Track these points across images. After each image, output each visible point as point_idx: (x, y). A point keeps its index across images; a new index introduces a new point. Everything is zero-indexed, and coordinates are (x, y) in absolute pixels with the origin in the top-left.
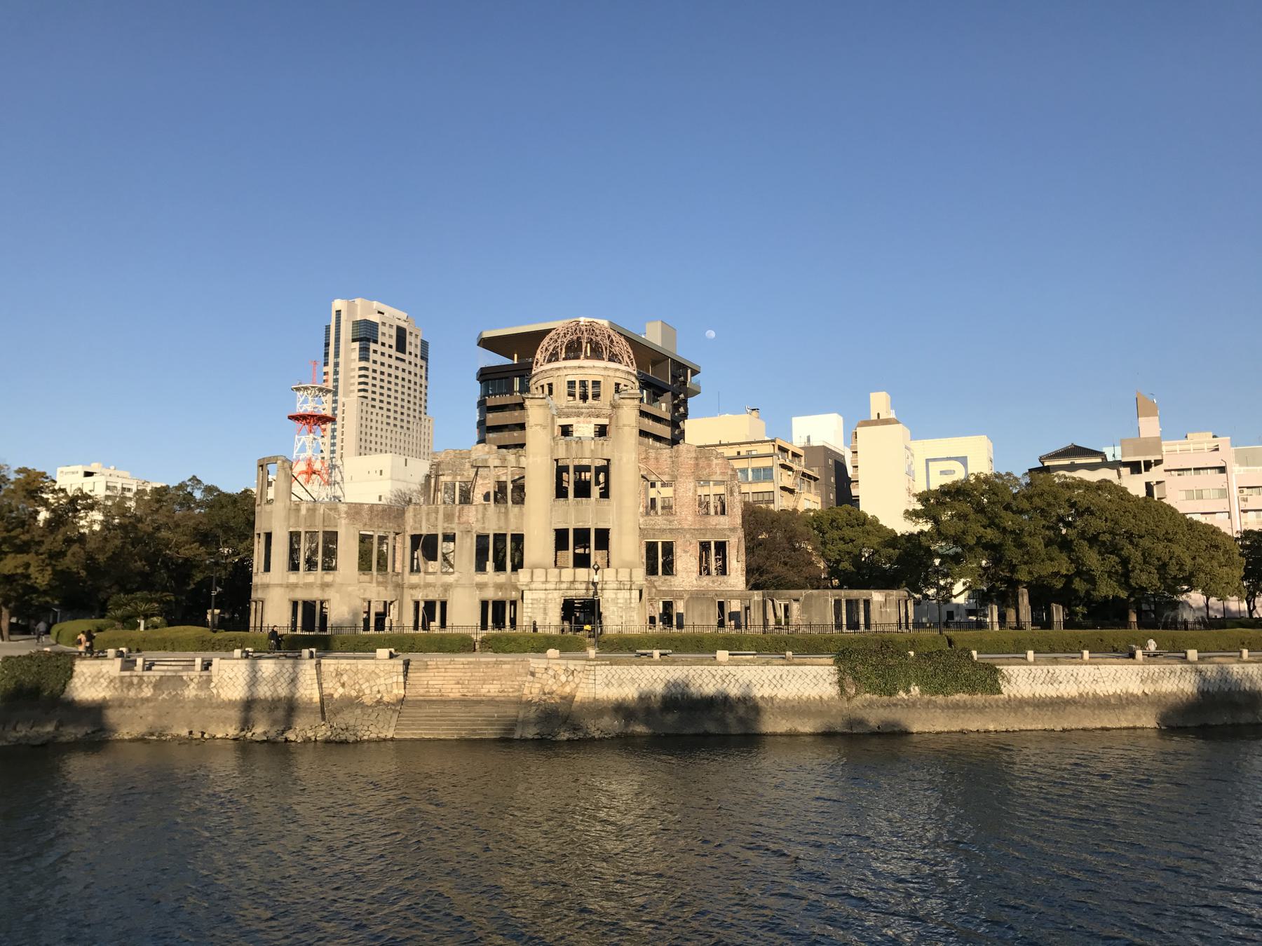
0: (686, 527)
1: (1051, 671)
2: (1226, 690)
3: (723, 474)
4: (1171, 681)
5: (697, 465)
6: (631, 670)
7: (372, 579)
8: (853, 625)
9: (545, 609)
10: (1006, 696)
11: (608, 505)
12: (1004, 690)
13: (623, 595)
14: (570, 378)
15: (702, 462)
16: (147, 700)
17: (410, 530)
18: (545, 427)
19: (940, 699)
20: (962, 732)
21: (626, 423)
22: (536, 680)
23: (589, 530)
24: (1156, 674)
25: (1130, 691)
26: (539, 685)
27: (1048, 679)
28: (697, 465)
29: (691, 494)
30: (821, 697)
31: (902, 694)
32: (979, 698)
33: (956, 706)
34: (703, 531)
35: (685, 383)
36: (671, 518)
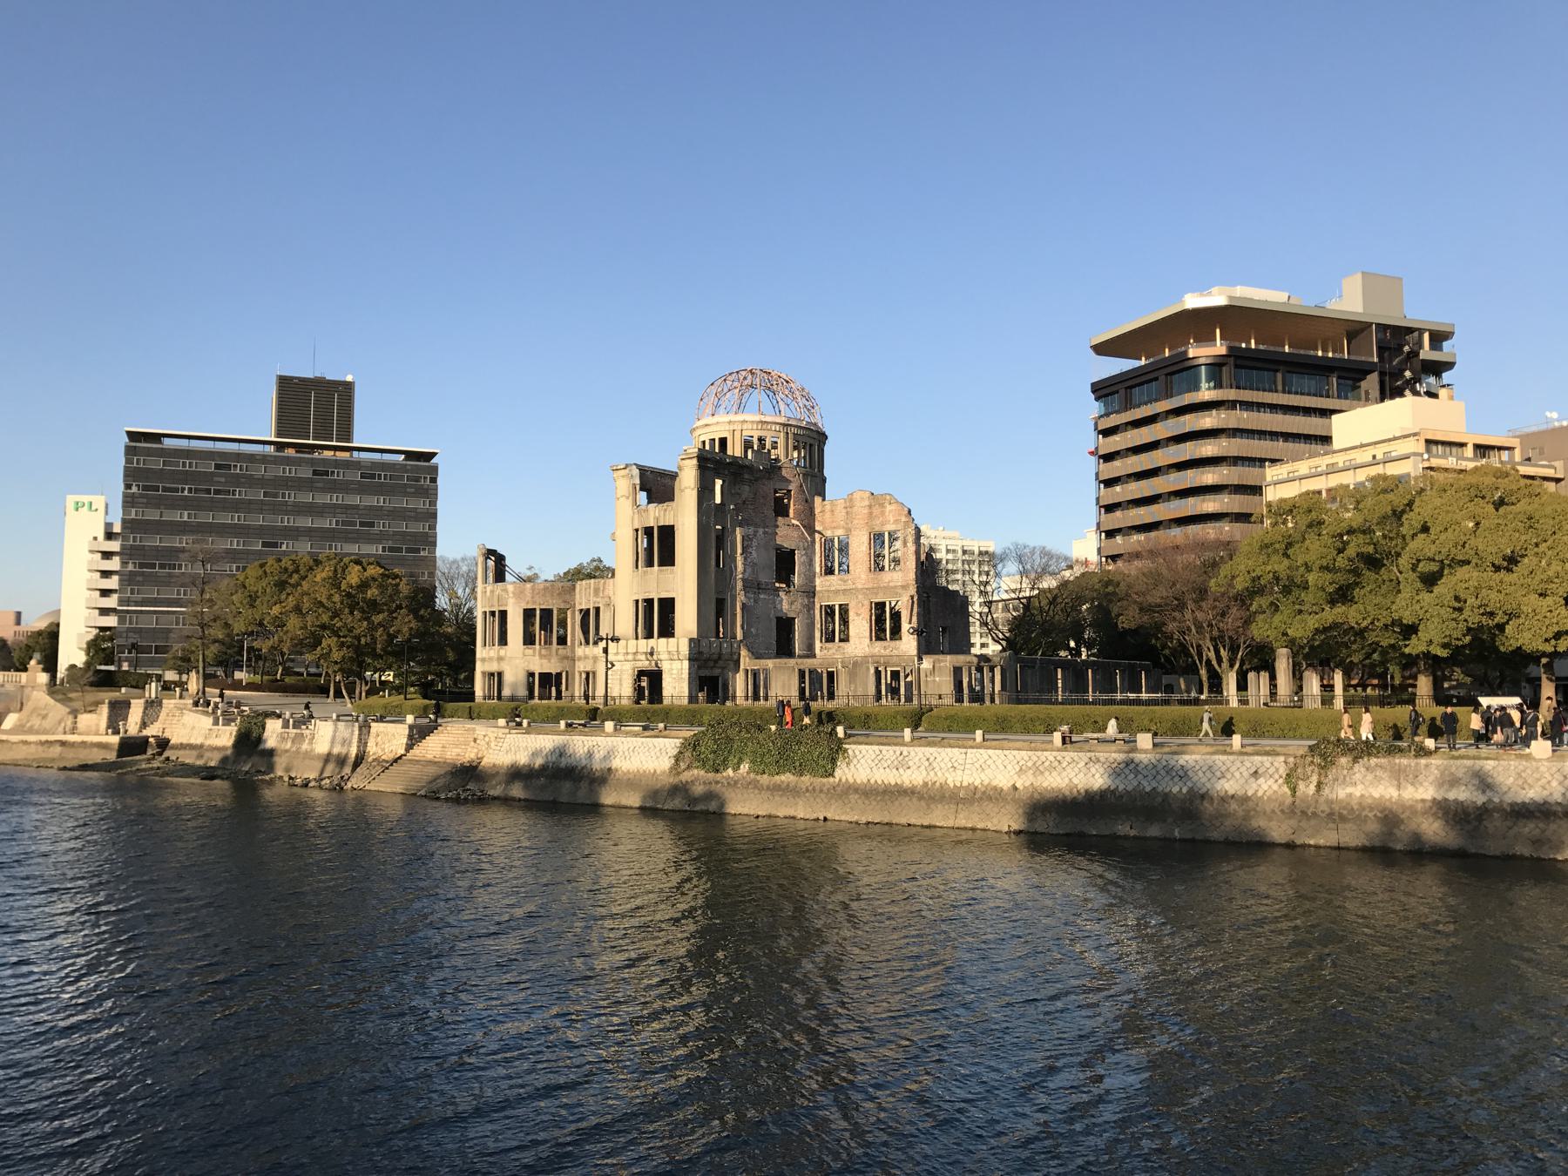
0: (860, 586)
1: (905, 753)
2: (1148, 789)
3: (896, 521)
4: (1064, 774)
5: (871, 513)
6: (529, 740)
7: (534, 652)
8: (756, 697)
9: (620, 680)
10: (837, 780)
11: (672, 572)
12: (836, 774)
13: (677, 665)
14: (702, 439)
15: (876, 510)
16: (287, 751)
17: (578, 607)
18: (628, 498)
19: (765, 779)
20: (770, 816)
21: (687, 485)
22: (476, 745)
23: (653, 599)
24: (1047, 764)
25: (994, 783)
26: (476, 750)
27: (896, 763)
28: (871, 513)
29: (864, 549)
30: (655, 771)
31: (730, 772)
32: (806, 779)
33: (776, 789)
34: (875, 590)
35: (1414, 354)
36: (846, 577)
